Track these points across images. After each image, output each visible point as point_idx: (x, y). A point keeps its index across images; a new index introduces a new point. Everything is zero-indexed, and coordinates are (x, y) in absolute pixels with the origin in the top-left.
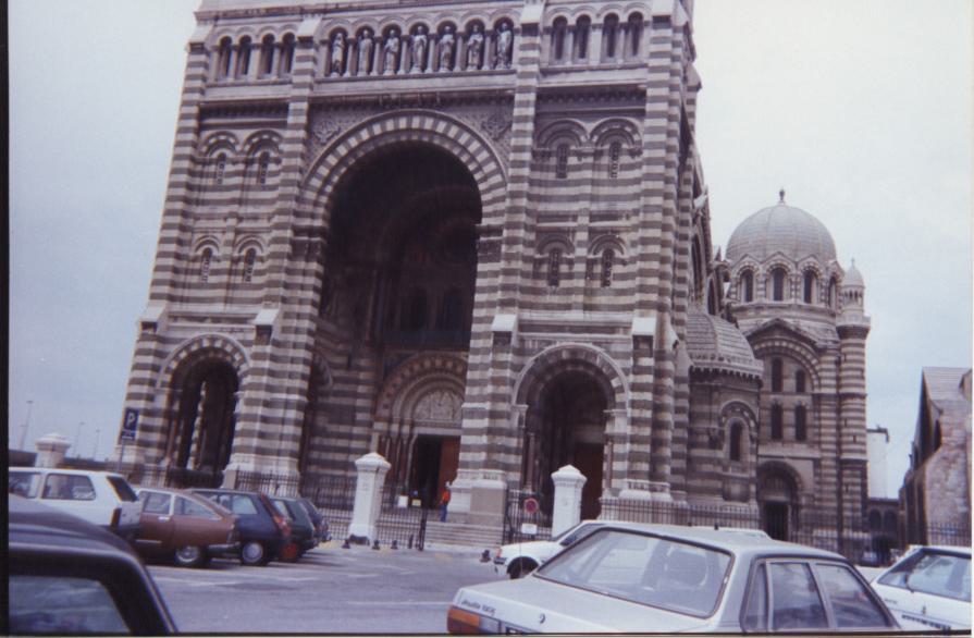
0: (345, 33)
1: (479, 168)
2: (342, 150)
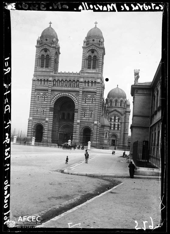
1: (75, 101)
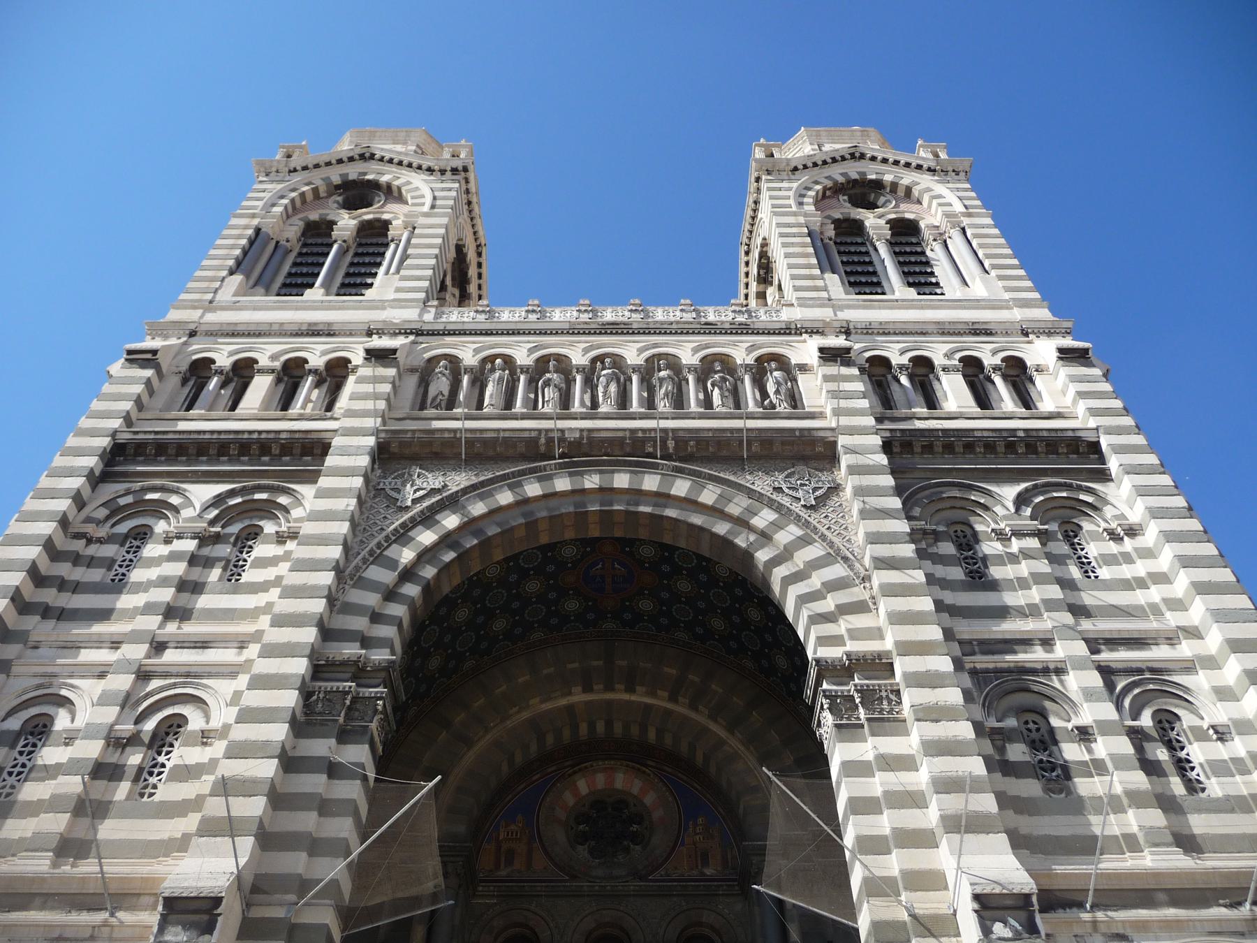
2: (451, 521)
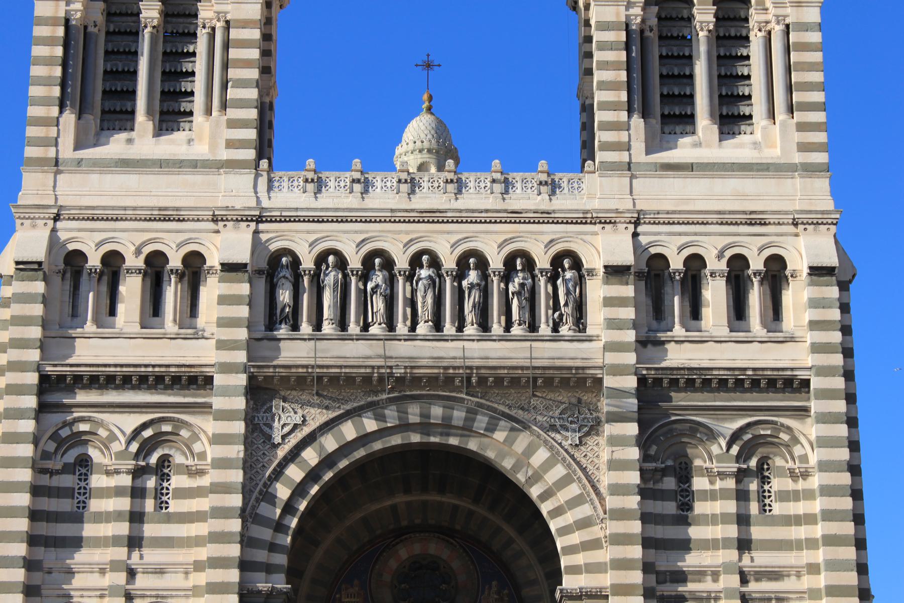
0: (296, 262)
2: (311, 456)
